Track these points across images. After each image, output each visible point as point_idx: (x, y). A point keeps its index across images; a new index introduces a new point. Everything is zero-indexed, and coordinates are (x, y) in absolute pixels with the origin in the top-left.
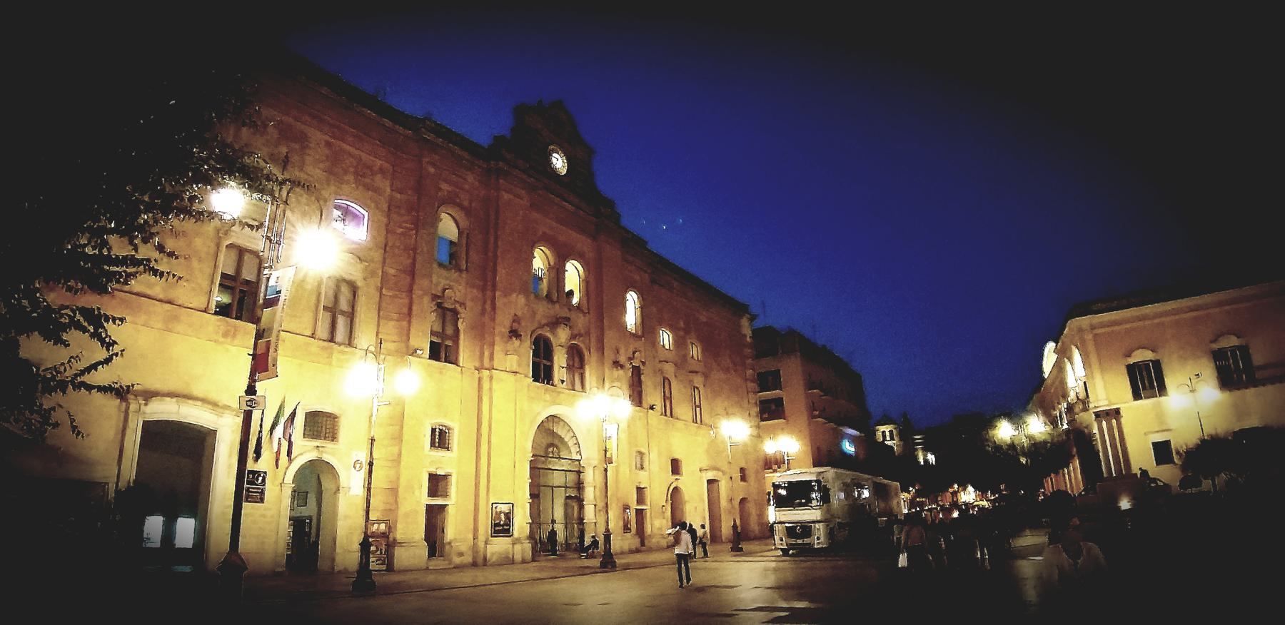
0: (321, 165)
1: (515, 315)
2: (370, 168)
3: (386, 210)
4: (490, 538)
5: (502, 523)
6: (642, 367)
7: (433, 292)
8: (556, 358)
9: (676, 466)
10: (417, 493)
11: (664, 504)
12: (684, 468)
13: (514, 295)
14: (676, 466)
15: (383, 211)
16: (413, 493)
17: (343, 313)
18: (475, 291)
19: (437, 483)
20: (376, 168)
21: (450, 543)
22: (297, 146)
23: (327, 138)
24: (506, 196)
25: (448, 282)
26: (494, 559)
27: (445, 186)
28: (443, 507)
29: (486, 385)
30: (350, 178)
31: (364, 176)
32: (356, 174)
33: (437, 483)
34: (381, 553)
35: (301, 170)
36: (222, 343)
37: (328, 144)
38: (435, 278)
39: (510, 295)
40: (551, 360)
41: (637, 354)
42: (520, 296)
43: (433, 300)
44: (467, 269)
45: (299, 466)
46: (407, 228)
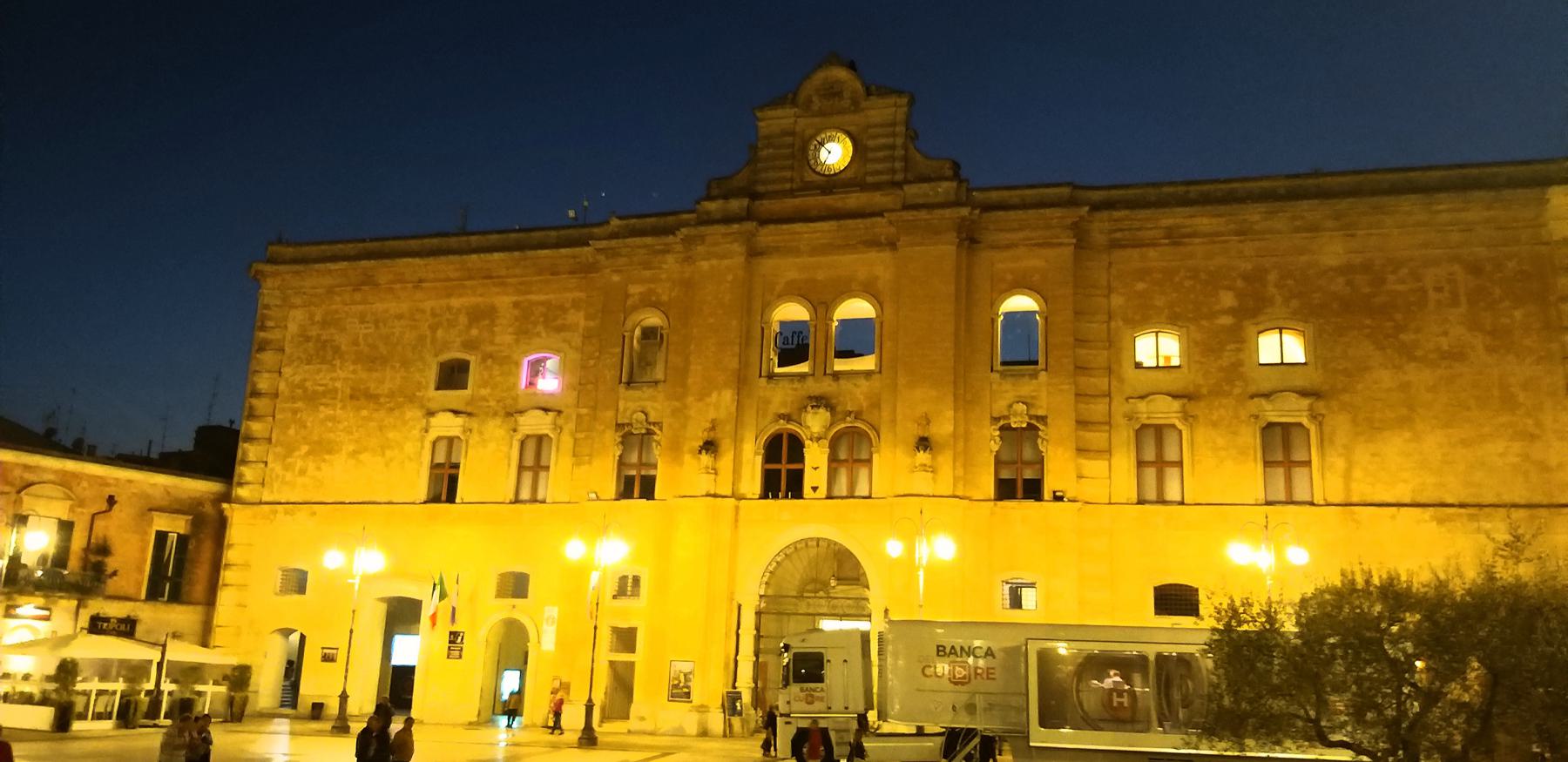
5: (681, 685)
7: (619, 422)
13: (714, 396)
15: (577, 349)
17: (529, 468)
24: (705, 265)
25: (638, 404)
27: (635, 289)
28: (631, 665)
30: (540, 328)
32: (546, 323)
35: (492, 343)
38: (621, 405)
39: (709, 395)
43: (616, 431)
45: (1189, 584)
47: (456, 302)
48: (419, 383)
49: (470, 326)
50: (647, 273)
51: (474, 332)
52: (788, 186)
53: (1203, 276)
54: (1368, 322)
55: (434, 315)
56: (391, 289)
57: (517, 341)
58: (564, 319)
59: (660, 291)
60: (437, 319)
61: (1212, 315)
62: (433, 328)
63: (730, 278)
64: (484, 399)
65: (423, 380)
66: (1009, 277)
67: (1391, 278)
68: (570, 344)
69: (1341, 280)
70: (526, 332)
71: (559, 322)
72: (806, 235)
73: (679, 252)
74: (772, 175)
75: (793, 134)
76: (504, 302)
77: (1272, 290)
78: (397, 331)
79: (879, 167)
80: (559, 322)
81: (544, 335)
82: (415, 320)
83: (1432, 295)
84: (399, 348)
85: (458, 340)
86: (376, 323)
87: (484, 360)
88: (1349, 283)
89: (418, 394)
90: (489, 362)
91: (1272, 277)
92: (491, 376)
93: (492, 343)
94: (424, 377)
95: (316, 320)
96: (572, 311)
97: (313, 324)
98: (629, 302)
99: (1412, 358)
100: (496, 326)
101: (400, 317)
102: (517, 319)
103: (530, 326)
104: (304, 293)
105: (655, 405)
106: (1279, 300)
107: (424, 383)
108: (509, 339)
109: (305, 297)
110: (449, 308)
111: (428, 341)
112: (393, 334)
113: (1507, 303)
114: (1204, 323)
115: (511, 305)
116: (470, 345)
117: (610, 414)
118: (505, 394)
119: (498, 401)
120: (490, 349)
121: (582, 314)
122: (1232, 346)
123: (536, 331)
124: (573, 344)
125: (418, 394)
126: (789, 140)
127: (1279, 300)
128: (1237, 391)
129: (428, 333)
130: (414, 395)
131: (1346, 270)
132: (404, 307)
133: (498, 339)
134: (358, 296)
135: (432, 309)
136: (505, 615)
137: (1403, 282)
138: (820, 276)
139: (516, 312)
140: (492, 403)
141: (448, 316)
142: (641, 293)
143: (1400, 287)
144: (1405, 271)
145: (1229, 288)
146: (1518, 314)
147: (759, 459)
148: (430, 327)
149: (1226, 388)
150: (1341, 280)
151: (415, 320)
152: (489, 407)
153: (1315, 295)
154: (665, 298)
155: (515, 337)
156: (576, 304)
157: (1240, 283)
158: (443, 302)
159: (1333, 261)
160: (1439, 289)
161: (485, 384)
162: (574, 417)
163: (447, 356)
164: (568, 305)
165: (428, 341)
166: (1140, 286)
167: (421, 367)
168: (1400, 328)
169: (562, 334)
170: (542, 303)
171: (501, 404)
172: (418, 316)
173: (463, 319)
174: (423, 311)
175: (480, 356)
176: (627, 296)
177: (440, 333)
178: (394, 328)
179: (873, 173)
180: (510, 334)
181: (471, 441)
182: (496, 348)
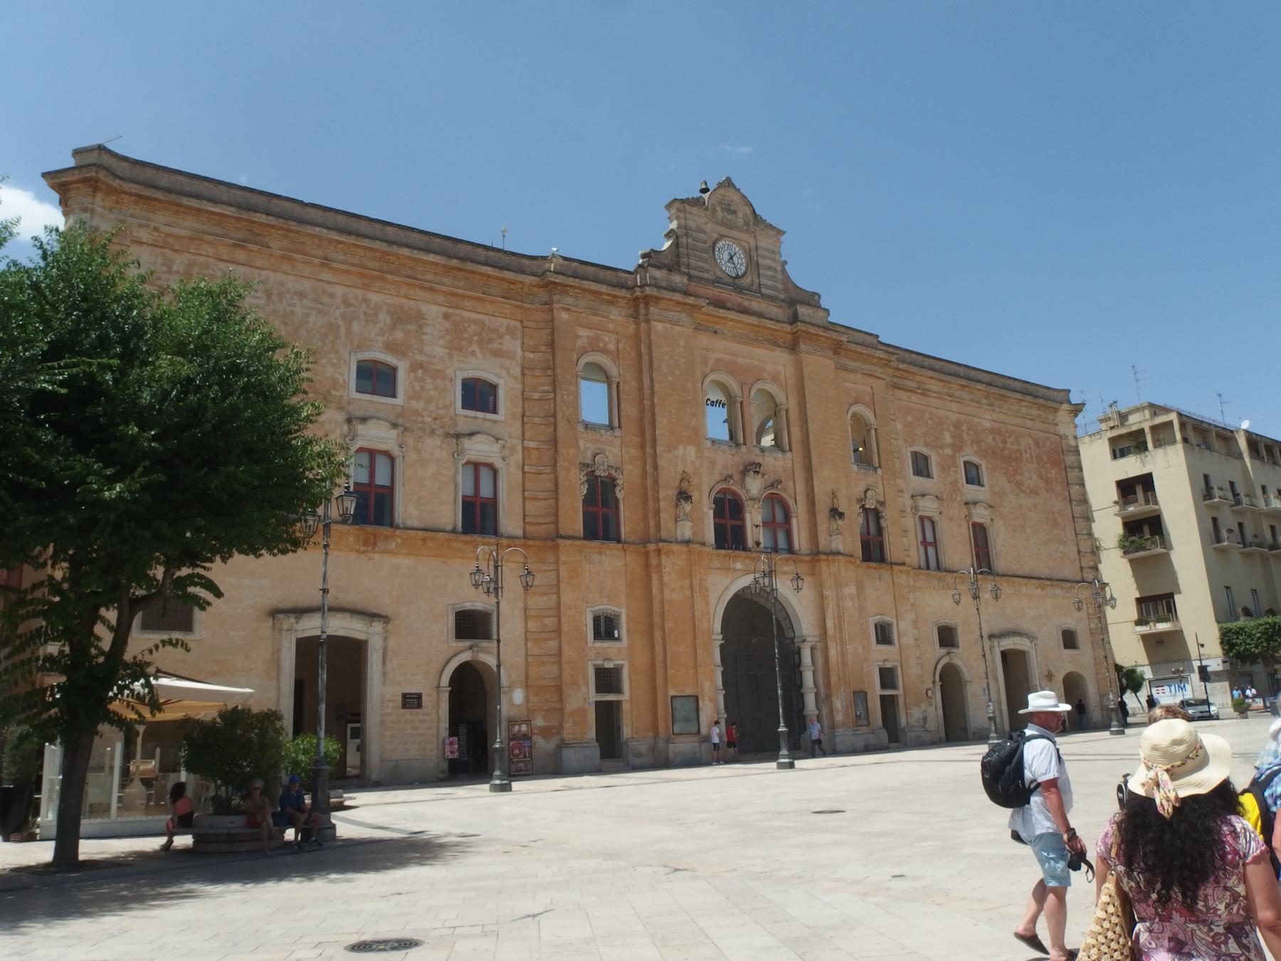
0: (442, 342)
1: (684, 472)
2: (495, 331)
3: (519, 375)
4: (673, 737)
6: (880, 509)
7: (582, 461)
8: (748, 516)
9: (947, 637)
10: (583, 689)
11: (930, 685)
12: (962, 638)
13: (681, 447)
14: (947, 637)
15: (516, 378)
16: (579, 689)
18: (632, 450)
19: (607, 679)
20: (503, 330)
21: (626, 742)
22: (413, 327)
23: (444, 309)
24: (659, 327)
26: (678, 760)
27: (584, 332)
29: (654, 561)
30: (475, 348)
31: (490, 341)
32: (481, 343)
33: (607, 679)
34: (525, 757)
35: (421, 352)
36: (364, 552)
37: (446, 316)
38: (581, 443)
39: (676, 448)
40: (743, 519)
41: (869, 494)
42: (688, 447)
43: (581, 470)
44: (620, 427)
46: (543, 392)
47: (375, 298)
48: (335, 380)
49: (393, 328)
50: (595, 319)
51: (399, 335)
52: (706, 276)
53: (936, 420)
54: (1004, 465)
55: (346, 303)
56: (290, 259)
57: (451, 356)
58: (500, 344)
59: (606, 339)
60: (351, 309)
61: (942, 447)
62: (348, 319)
63: (682, 343)
64: (417, 413)
65: (338, 376)
66: (853, 394)
67: (1009, 440)
68: (508, 372)
69: (991, 437)
70: (460, 349)
71: (495, 346)
72: (731, 323)
73: (622, 307)
74: (693, 262)
75: (704, 232)
76: (432, 311)
77: (965, 436)
78: (299, 311)
79: (770, 283)
80: (495, 346)
81: (479, 355)
82: (321, 303)
83: (1025, 456)
84: (303, 332)
85: (380, 338)
86: (268, 294)
87: (415, 367)
88: (994, 439)
89: (334, 392)
90: (420, 372)
91: (965, 428)
92: (423, 388)
93: (421, 352)
94: (341, 374)
95: (175, 268)
96: (507, 338)
97: (170, 272)
98: (579, 343)
99: (1021, 491)
100: (425, 334)
101: (301, 295)
102: (447, 332)
103: (464, 343)
104: (156, 229)
105: (612, 449)
106: (968, 443)
107: (341, 381)
108: (440, 351)
109: (156, 234)
110: (366, 301)
111: (343, 330)
112: (293, 313)
113: (1048, 466)
114: (941, 452)
115: (440, 315)
116: (391, 348)
117: (572, 451)
118: (443, 412)
119: (435, 419)
120: (419, 358)
121: (518, 343)
122: (953, 469)
123: (470, 350)
124: (512, 372)
125: (334, 392)
126: (702, 236)
127: (968, 443)
128: (959, 499)
129: (340, 322)
130: (329, 392)
131: (992, 431)
132: (306, 286)
133: (427, 349)
134: (240, 255)
135: (344, 295)
136: (465, 657)
137: (1012, 443)
138: (740, 361)
139: (447, 324)
140: (428, 419)
141: (364, 308)
142: (588, 337)
143: (1014, 447)
144: (1013, 438)
145: (948, 431)
146: (1053, 472)
147: (711, 513)
148: (343, 317)
149: (954, 496)
150: (991, 437)
151: (321, 303)
152: (423, 422)
153: (983, 444)
154: (612, 347)
155: (447, 351)
156: (511, 332)
157: (952, 429)
158: (360, 293)
159: (987, 425)
160: (1026, 452)
161: (416, 396)
162: (520, 447)
163: (367, 355)
164: (503, 330)
165: (343, 330)
166: (909, 418)
167: (335, 361)
168: (1016, 472)
169: (499, 359)
170: (475, 322)
171: (438, 422)
172: (325, 299)
173: (385, 319)
174: (332, 296)
175: (408, 363)
176: (578, 337)
177: (356, 326)
178: (294, 305)
179: (767, 287)
180: (442, 346)
181: (407, 459)
182: (426, 359)
